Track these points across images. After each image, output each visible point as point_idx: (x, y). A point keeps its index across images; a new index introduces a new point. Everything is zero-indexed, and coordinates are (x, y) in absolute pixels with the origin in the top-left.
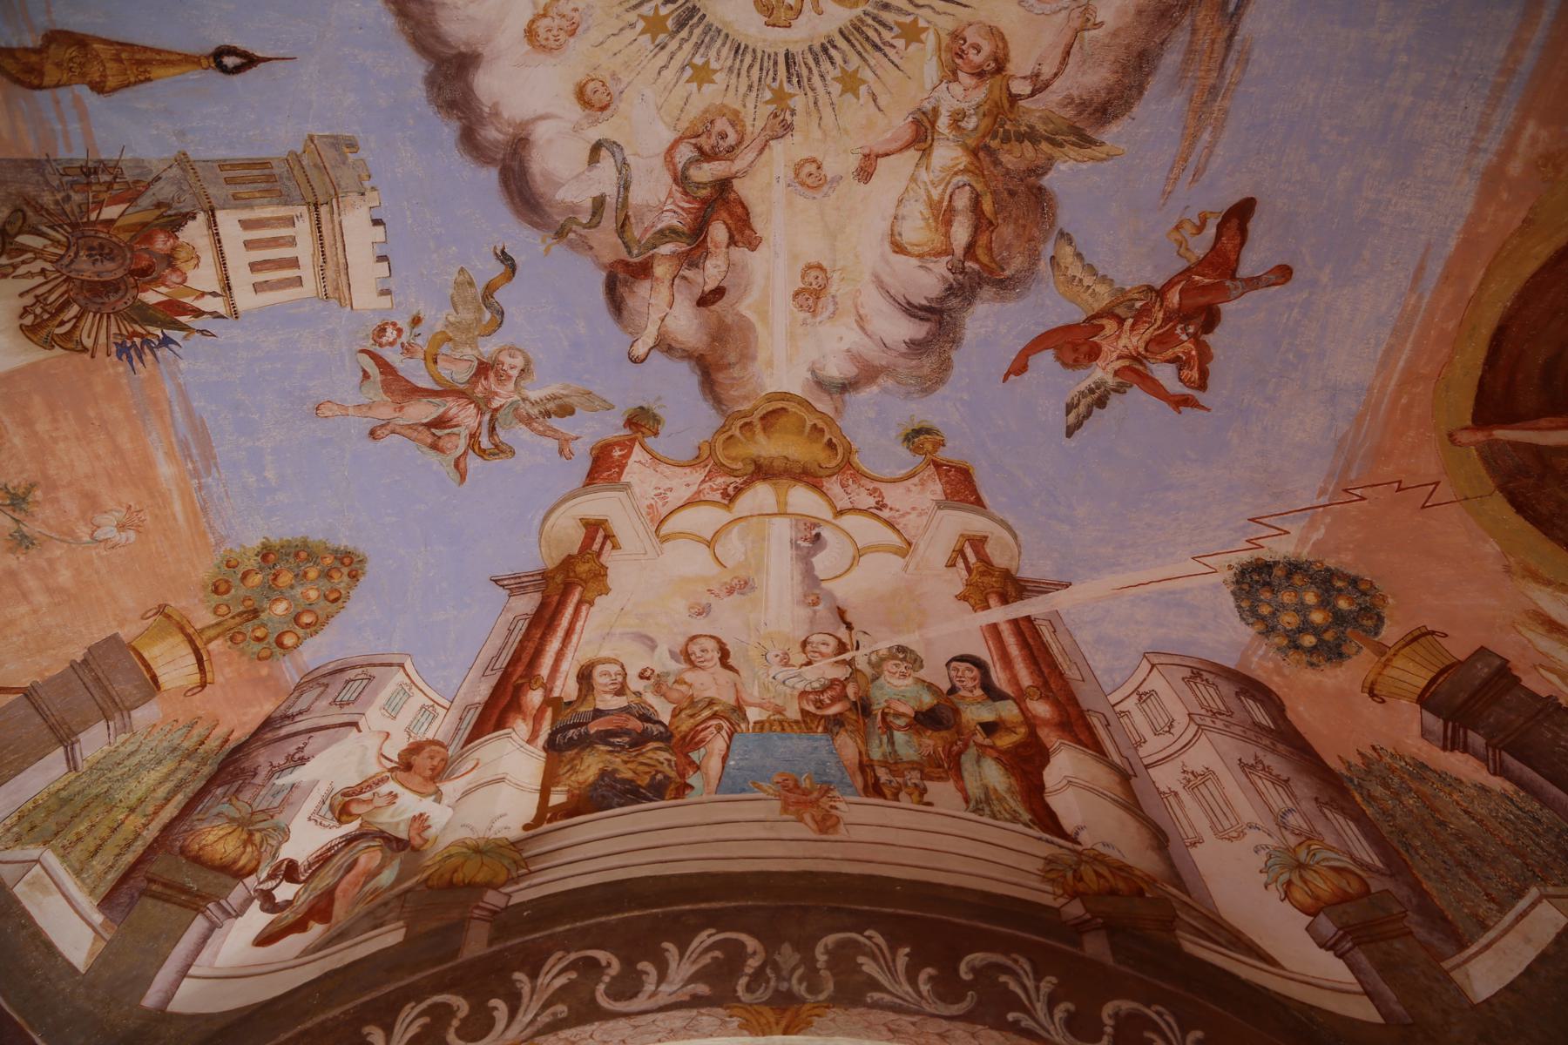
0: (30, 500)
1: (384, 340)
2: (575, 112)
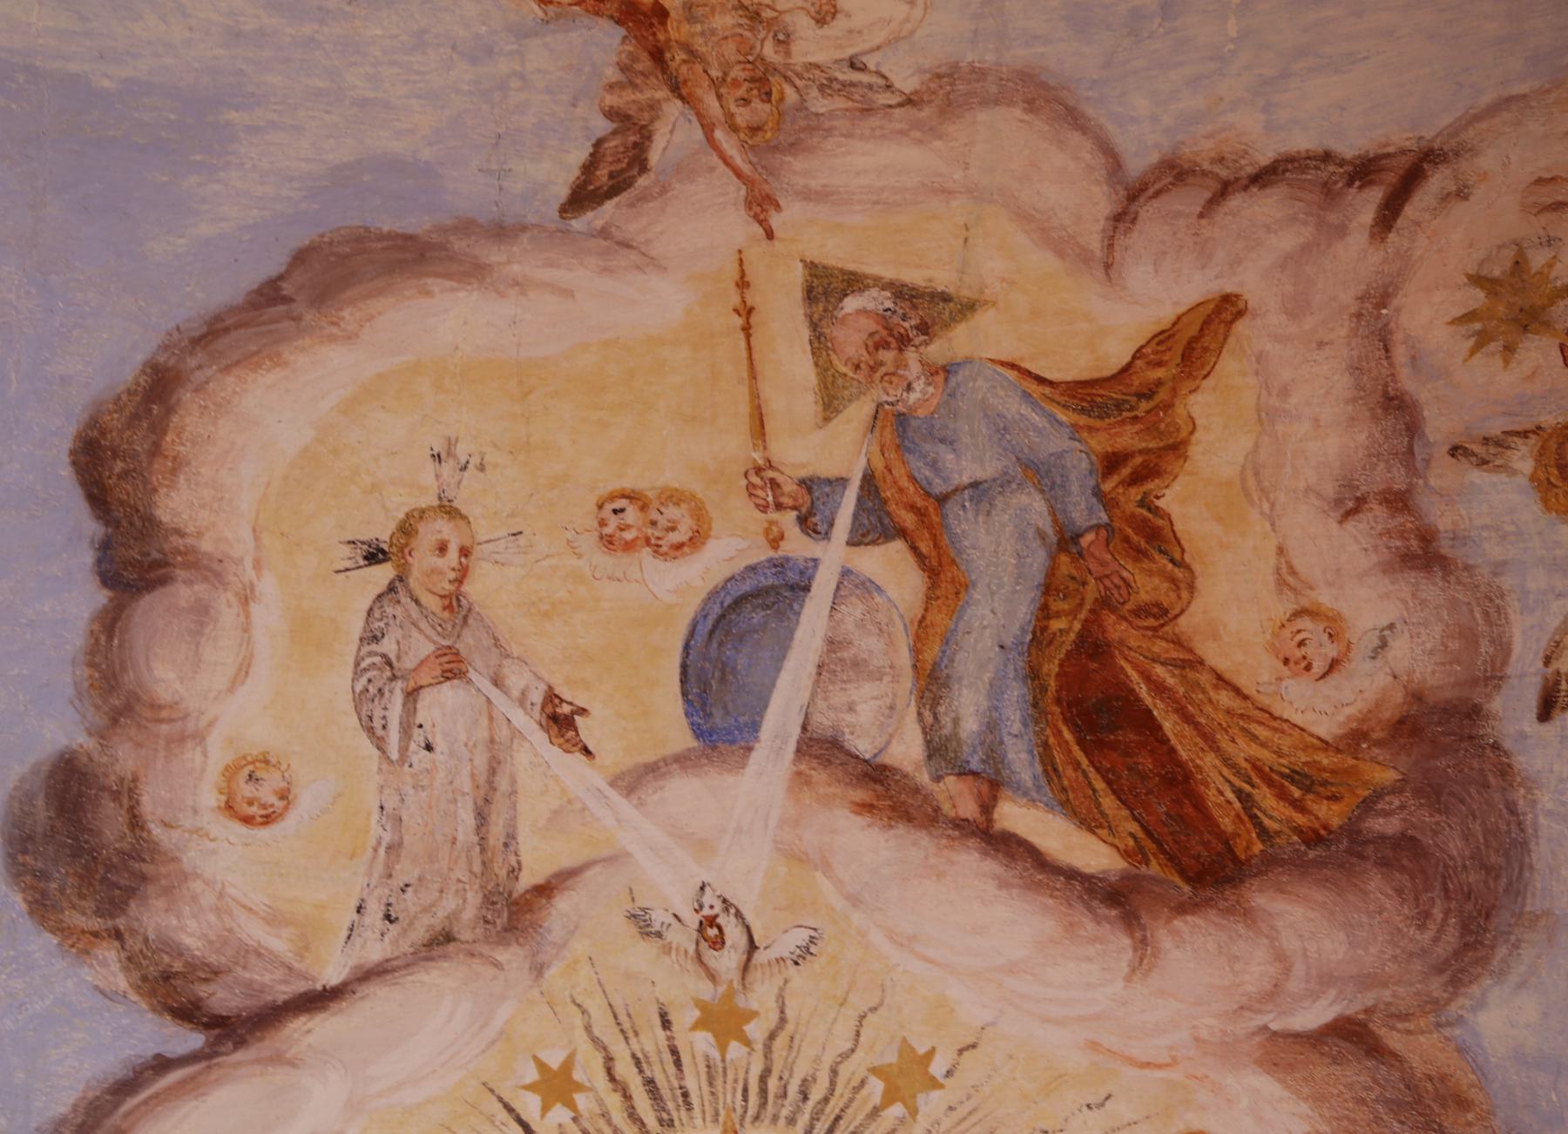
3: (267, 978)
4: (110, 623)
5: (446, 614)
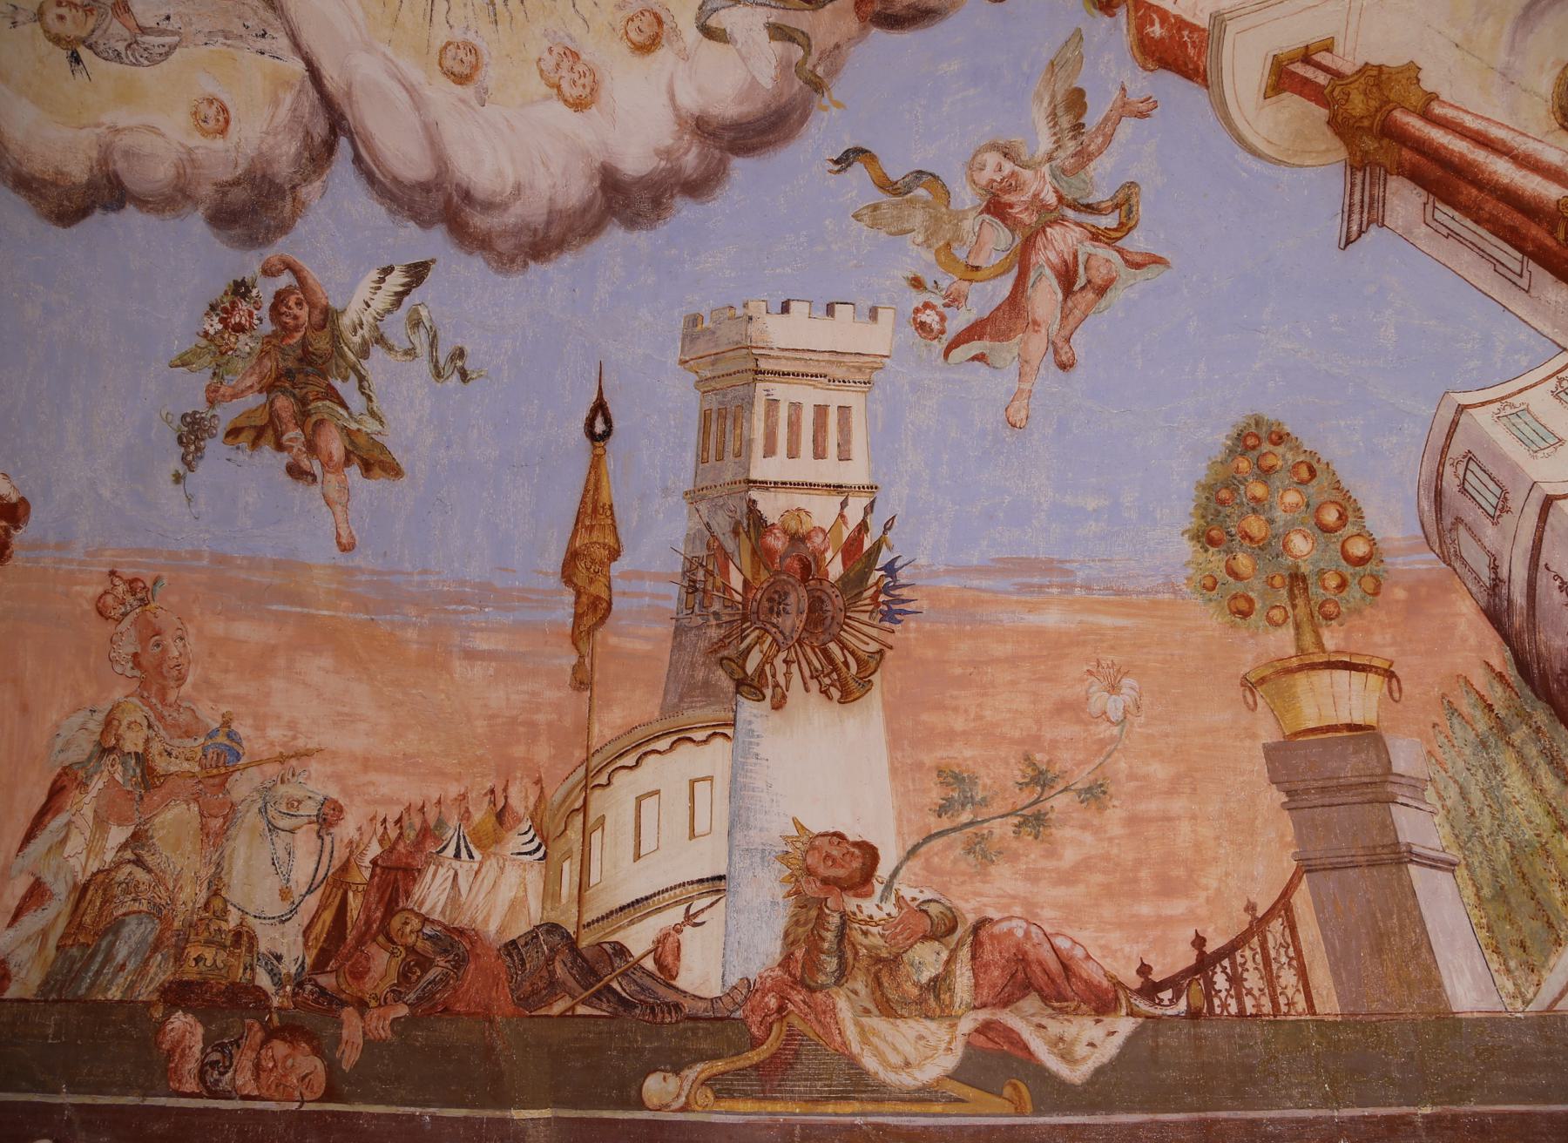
0: (1044, 767)
1: (936, 327)
2: (664, 56)
3: (307, 104)
4: (142, 203)
5: (95, 12)
